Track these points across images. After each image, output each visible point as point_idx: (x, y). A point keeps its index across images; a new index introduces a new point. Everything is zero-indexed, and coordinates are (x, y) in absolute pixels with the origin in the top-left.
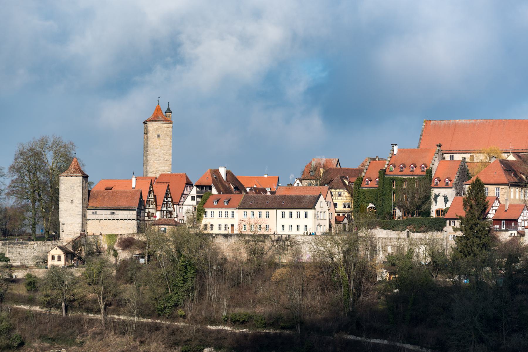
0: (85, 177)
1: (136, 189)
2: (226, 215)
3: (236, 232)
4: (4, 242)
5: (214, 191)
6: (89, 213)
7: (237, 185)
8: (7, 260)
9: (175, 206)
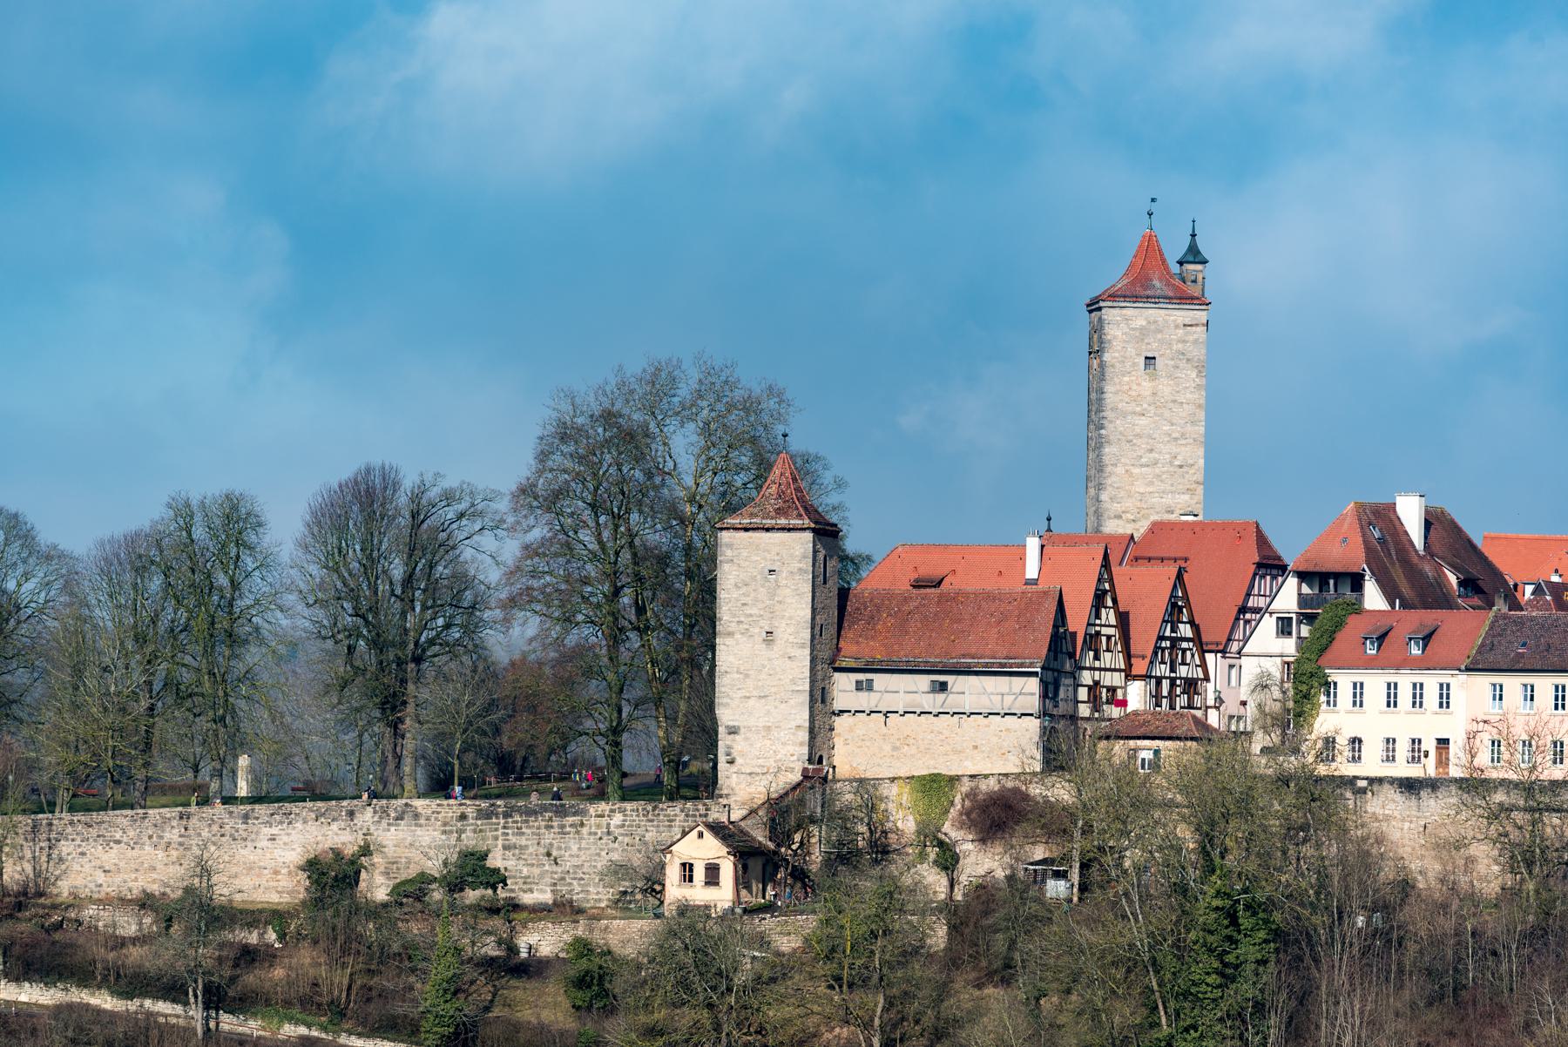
0: (826, 533)
1: (1040, 587)
2: (1417, 700)
3: (1455, 772)
4: (484, 804)
5: (1373, 598)
6: (843, 687)
7: (1475, 572)
8: (496, 879)
9: (1210, 657)
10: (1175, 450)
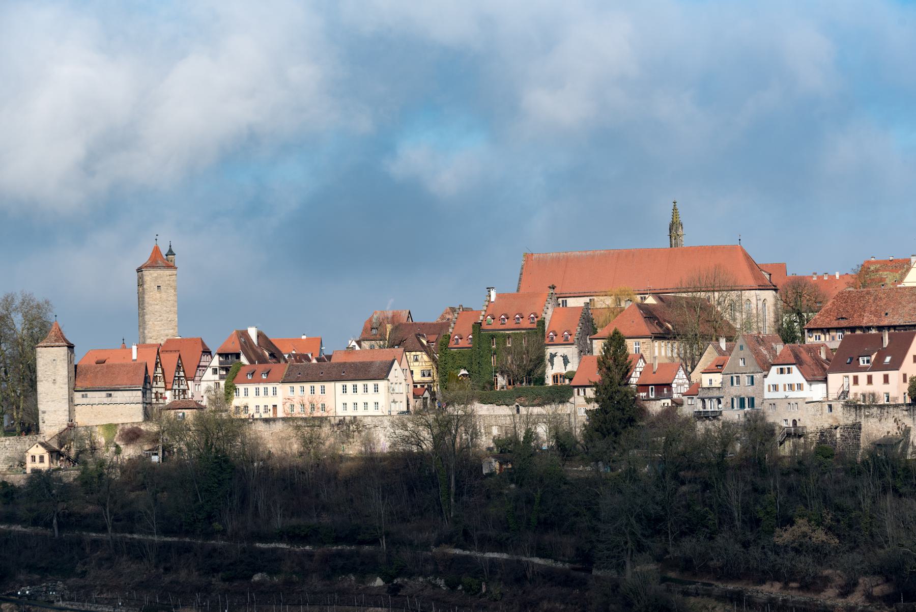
0: (71, 347)
2: (266, 393)
3: (280, 414)
5: (243, 359)
6: (78, 396)
9: (189, 382)
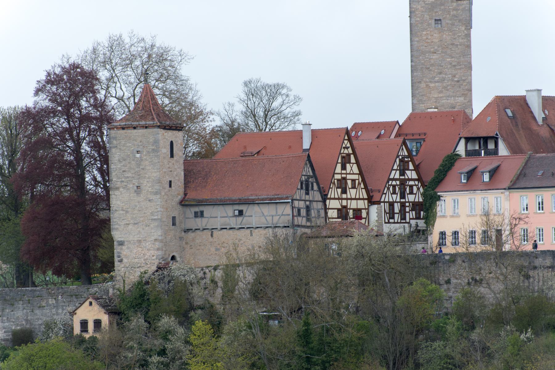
10: (454, 72)
